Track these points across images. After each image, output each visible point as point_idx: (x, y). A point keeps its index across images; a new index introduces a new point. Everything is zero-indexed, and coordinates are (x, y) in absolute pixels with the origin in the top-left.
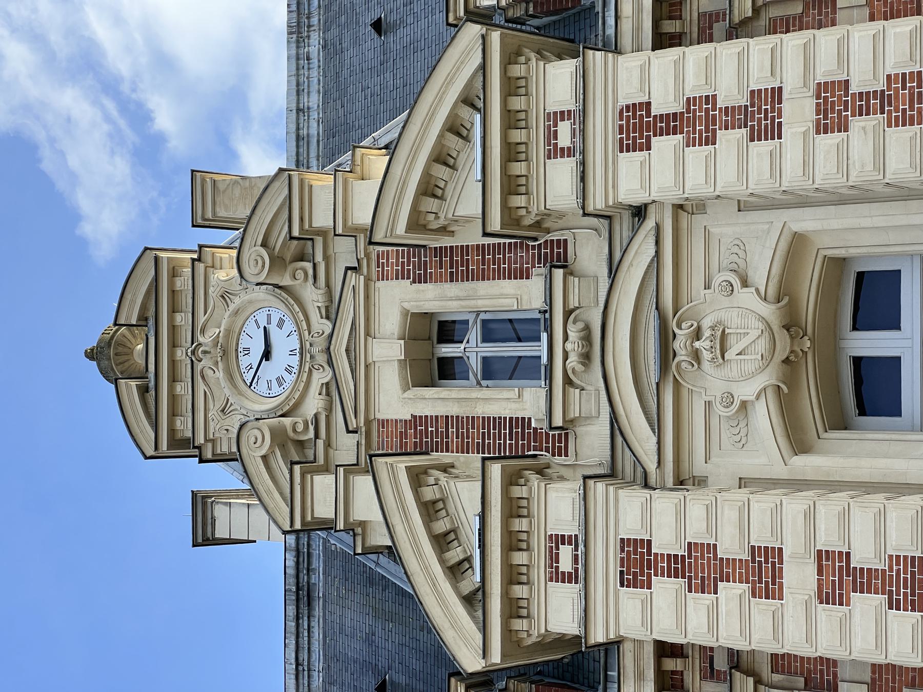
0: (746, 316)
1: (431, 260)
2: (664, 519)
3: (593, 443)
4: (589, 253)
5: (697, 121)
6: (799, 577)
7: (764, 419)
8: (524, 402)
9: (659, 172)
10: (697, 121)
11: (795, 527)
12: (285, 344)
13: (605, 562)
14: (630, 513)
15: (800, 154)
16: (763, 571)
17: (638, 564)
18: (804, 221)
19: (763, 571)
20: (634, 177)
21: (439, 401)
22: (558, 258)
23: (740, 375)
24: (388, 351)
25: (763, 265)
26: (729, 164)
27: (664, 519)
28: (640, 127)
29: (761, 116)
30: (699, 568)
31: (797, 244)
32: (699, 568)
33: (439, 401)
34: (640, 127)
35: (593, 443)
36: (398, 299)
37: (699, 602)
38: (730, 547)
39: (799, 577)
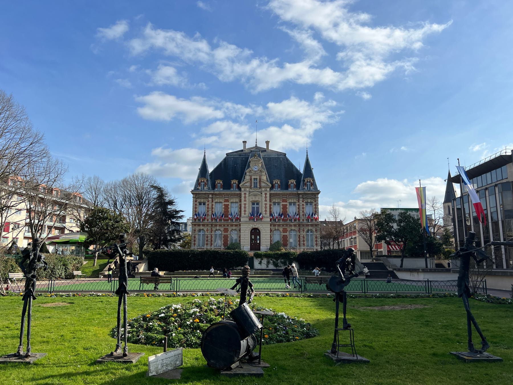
0: (257, 199)
1: (260, 179)
3: (251, 190)
4: (260, 190)
5: (266, 197)
6: (245, 202)
8: (253, 187)
9: (264, 195)
10: (266, 197)
11: (247, 202)
12: (256, 170)
14: (247, 193)
15: (264, 202)
16: (245, 201)
17: (245, 194)
19: (245, 201)
20: (263, 194)
21: (253, 180)
22: (260, 188)
23: (254, 199)
26: (264, 199)
27: (247, 195)
28: (266, 194)
29: (266, 201)
30: (245, 197)
32: (245, 197)
33: (253, 180)
34: (266, 194)
35: (251, 190)
36: (258, 177)
39: (245, 202)
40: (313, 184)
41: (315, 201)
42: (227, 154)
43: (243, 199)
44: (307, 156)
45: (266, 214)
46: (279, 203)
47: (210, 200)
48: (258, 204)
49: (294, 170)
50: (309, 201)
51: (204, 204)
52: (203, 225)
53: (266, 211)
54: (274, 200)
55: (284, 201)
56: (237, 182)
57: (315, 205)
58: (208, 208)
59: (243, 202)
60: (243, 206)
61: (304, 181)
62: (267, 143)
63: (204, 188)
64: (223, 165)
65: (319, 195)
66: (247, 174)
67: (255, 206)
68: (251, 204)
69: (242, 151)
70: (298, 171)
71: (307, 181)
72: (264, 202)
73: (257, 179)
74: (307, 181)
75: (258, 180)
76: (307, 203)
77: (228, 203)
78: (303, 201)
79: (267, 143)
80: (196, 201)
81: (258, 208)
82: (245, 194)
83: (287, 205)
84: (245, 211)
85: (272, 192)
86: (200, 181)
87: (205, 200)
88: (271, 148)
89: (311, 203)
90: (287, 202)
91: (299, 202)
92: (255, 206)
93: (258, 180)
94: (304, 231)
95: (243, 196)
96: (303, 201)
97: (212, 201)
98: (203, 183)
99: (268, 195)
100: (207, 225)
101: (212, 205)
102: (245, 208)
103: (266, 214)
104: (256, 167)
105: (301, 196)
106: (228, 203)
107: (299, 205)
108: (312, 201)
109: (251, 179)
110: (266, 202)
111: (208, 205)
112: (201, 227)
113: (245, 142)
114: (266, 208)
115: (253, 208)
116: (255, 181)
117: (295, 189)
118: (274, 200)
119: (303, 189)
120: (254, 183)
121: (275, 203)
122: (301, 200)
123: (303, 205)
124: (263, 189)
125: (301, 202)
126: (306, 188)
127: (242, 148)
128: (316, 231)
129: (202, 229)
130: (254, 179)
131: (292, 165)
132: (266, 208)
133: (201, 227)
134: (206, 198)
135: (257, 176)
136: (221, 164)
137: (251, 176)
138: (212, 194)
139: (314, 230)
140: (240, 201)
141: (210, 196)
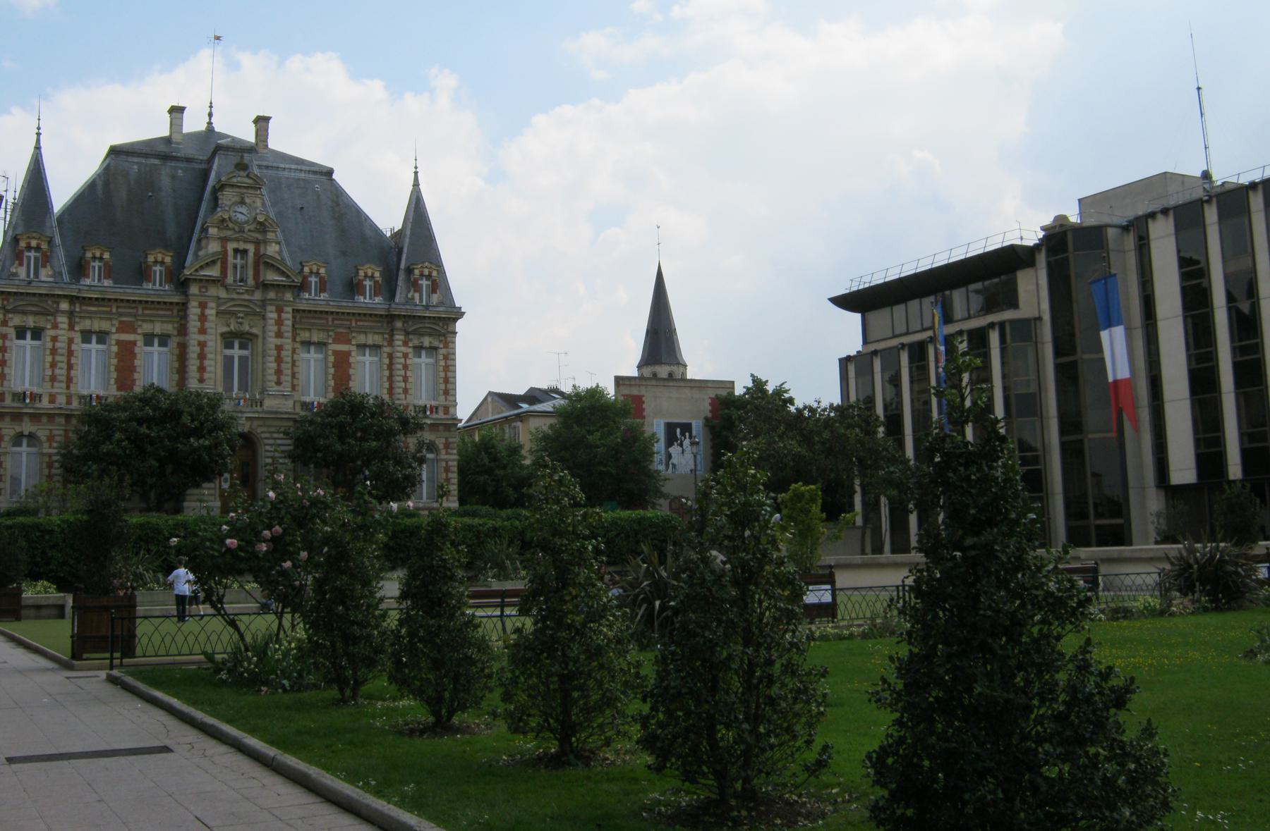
2: (211, 312)
5: (279, 322)
6: (202, 338)
7: (225, 329)
9: (272, 316)
10: (279, 322)
13: (203, 299)
16: (203, 331)
17: (203, 306)
18: (260, 340)
19: (203, 331)
21: (230, 253)
24: (242, 246)
25: (255, 330)
27: (211, 312)
29: (279, 335)
30: (203, 318)
31: (256, 336)
32: (203, 318)
33: (230, 253)
37: (196, 318)
38: (207, 325)
39: (202, 338)
40: (439, 283)
41: (446, 346)
42: (115, 152)
43: (193, 324)
45: (279, 383)
46: (321, 345)
47: (63, 320)
49: (368, 232)
50: (426, 344)
51: (37, 334)
52: (35, 417)
53: (279, 372)
54: (304, 335)
55: (338, 340)
56: (168, 260)
57: (446, 358)
58: (54, 351)
59: (194, 338)
60: (193, 351)
61: (409, 271)
62: (262, 122)
63: (37, 274)
64: (100, 188)
65: (459, 325)
66: (213, 231)
67: (236, 352)
69: (167, 141)
71: (422, 275)
72: (273, 341)
73: (245, 252)
74: (422, 275)
75: (251, 254)
76: (418, 349)
77: (131, 337)
78: (405, 344)
79: (262, 122)
82: (203, 306)
83: (349, 353)
84: (202, 369)
86: (23, 244)
87: (42, 322)
88: (278, 142)
89: (433, 350)
90: (348, 342)
91: (391, 343)
92: (236, 352)
93: (251, 254)
95: (194, 310)
96: (405, 344)
97: (71, 327)
98: (32, 254)
99: (287, 316)
100: (51, 417)
101: (71, 341)
102: (202, 357)
103: (279, 383)
104: (243, 210)
105: (399, 324)
106: (131, 337)
107: (391, 356)
108: (436, 343)
109: (225, 253)
110: (279, 341)
111: (54, 339)
112: (27, 427)
113: (176, 111)
114: (279, 360)
115: (228, 361)
116: (239, 261)
117: (378, 300)
118: (304, 335)
119: (409, 301)
120: (235, 267)
121: (307, 344)
122: (399, 338)
123: (405, 356)
124: (271, 295)
125: (400, 348)
126: (417, 296)
127: (165, 132)
128: (447, 446)
129: (31, 436)
130: (236, 251)
131: (358, 212)
132: (279, 360)
133: (27, 427)
134: (46, 313)
135: (246, 241)
136: (91, 187)
137: (224, 240)
138: (72, 299)
139: (440, 443)
140: (183, 330)
141: (64, 306)
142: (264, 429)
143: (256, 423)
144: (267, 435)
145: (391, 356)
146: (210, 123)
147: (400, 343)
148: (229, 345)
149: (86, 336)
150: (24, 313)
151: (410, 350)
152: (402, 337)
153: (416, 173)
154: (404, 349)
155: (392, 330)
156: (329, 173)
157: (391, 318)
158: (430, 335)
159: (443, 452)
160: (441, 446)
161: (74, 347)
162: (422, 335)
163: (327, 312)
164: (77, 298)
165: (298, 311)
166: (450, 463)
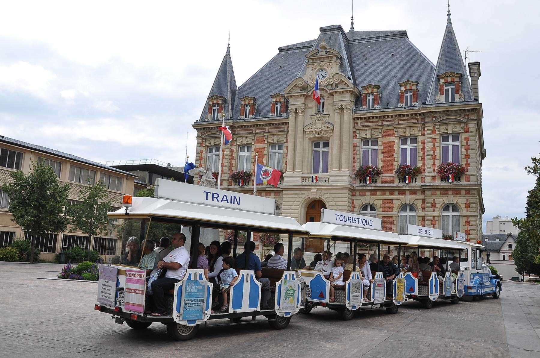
44: (449, 23)
48: (326, 145)
68: (308, 145)
70: (424, 61)
77: (262, 146)
78: (434, 132)
80: (202, 145)
81: (326, 154)
85: (359, 114)
90: (394, 135)
91: (423, 134)
92: (321, 149)
94: (434, 205)
96: (434, 132)
101: (232, 151)
105: (429, 119)
106: (262, 146)
108: (458, 129)
115: (317, 154)
122: (429, 127)
123: (434, 140)
142: (328, 195)
143: (323, 192)
144: (331, 199)
145: (423, 142)
146: (352, 28)
147: (429, 132)
148: (317, 145)
149: (241, 147)
150: (210, 138)
151: (437, 137)
152: (431, 128)
153: (449, 15)
154: (433, 136)
155: (423, 124)
156: (403, 34)
157: (423, 115)
158: (453, 124)
159: (465, 210)
160: (463, 206)
161: (234, 154)
162: (447, 125)
163: (377, 117)
164: (235, 127)
165: (358, 119)
166: (470, 218)
